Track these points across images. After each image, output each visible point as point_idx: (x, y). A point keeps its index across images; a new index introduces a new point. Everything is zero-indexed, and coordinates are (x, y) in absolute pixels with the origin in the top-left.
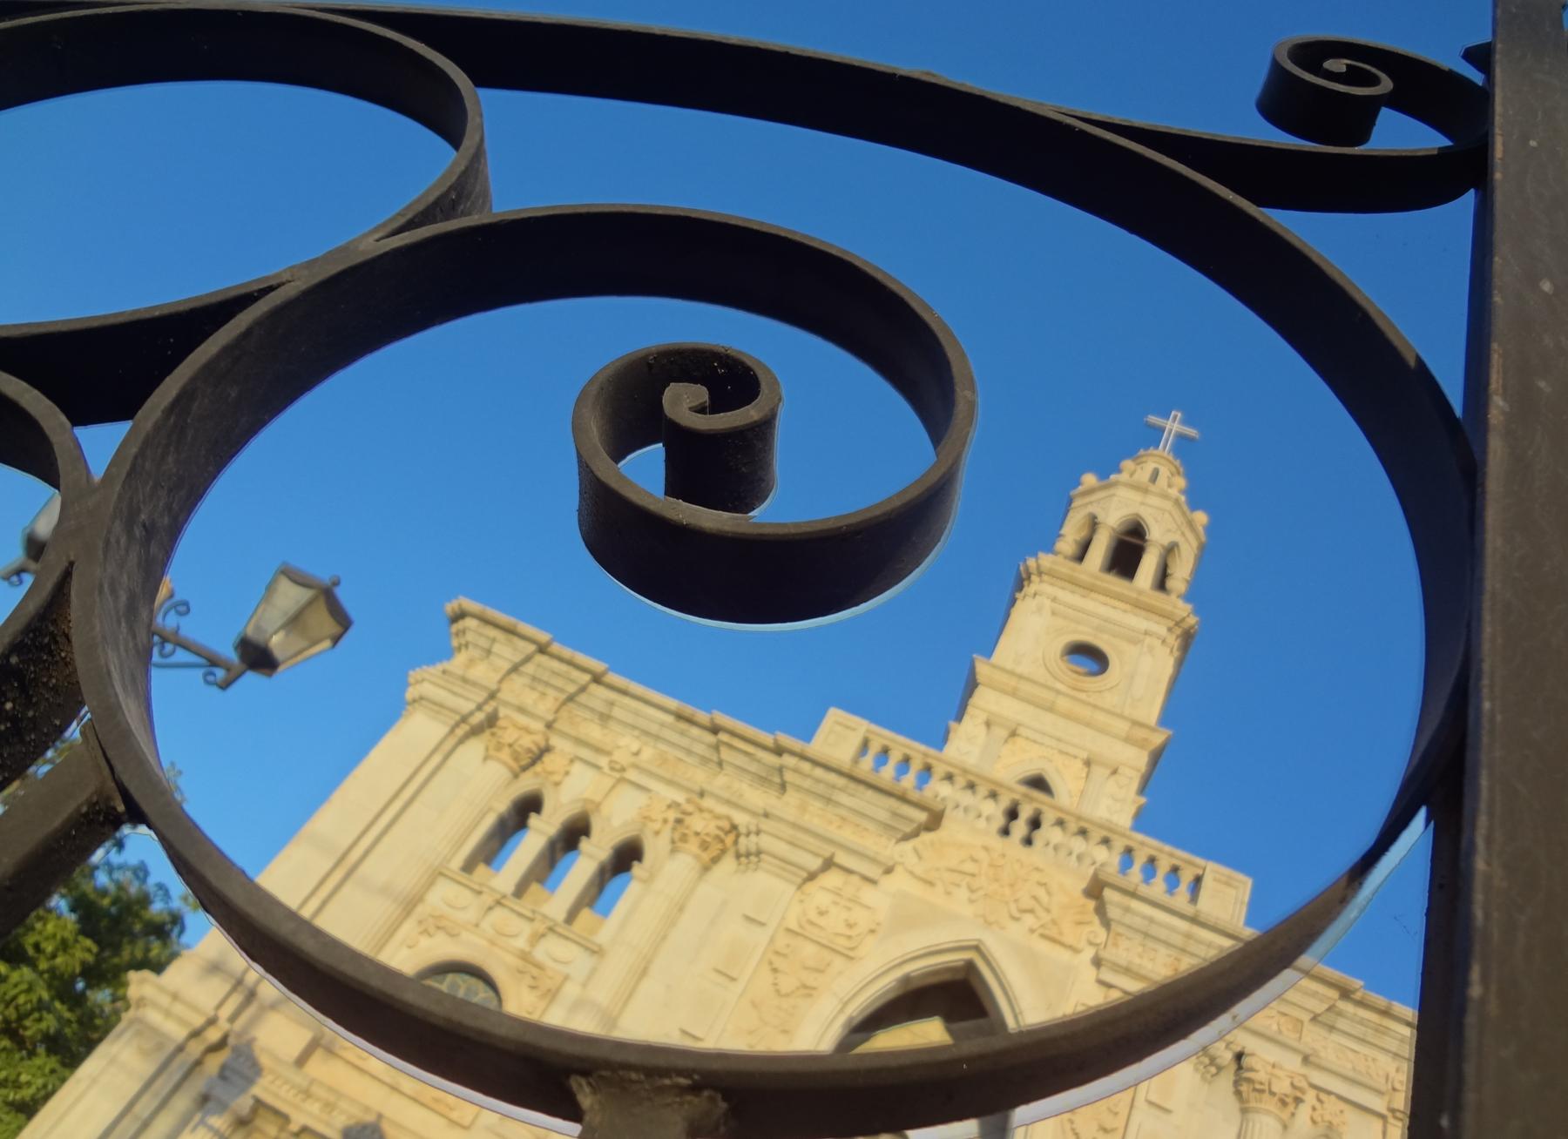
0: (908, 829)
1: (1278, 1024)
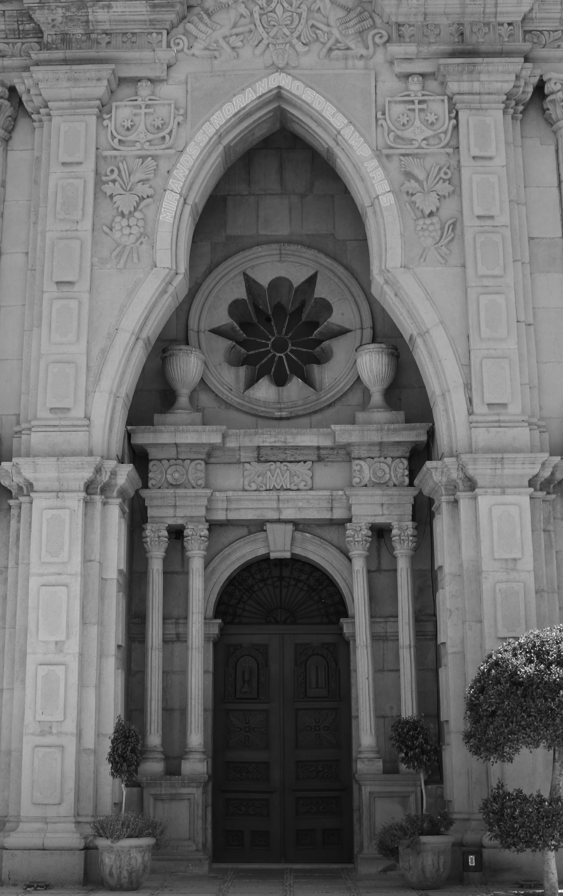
0: (172, 17)
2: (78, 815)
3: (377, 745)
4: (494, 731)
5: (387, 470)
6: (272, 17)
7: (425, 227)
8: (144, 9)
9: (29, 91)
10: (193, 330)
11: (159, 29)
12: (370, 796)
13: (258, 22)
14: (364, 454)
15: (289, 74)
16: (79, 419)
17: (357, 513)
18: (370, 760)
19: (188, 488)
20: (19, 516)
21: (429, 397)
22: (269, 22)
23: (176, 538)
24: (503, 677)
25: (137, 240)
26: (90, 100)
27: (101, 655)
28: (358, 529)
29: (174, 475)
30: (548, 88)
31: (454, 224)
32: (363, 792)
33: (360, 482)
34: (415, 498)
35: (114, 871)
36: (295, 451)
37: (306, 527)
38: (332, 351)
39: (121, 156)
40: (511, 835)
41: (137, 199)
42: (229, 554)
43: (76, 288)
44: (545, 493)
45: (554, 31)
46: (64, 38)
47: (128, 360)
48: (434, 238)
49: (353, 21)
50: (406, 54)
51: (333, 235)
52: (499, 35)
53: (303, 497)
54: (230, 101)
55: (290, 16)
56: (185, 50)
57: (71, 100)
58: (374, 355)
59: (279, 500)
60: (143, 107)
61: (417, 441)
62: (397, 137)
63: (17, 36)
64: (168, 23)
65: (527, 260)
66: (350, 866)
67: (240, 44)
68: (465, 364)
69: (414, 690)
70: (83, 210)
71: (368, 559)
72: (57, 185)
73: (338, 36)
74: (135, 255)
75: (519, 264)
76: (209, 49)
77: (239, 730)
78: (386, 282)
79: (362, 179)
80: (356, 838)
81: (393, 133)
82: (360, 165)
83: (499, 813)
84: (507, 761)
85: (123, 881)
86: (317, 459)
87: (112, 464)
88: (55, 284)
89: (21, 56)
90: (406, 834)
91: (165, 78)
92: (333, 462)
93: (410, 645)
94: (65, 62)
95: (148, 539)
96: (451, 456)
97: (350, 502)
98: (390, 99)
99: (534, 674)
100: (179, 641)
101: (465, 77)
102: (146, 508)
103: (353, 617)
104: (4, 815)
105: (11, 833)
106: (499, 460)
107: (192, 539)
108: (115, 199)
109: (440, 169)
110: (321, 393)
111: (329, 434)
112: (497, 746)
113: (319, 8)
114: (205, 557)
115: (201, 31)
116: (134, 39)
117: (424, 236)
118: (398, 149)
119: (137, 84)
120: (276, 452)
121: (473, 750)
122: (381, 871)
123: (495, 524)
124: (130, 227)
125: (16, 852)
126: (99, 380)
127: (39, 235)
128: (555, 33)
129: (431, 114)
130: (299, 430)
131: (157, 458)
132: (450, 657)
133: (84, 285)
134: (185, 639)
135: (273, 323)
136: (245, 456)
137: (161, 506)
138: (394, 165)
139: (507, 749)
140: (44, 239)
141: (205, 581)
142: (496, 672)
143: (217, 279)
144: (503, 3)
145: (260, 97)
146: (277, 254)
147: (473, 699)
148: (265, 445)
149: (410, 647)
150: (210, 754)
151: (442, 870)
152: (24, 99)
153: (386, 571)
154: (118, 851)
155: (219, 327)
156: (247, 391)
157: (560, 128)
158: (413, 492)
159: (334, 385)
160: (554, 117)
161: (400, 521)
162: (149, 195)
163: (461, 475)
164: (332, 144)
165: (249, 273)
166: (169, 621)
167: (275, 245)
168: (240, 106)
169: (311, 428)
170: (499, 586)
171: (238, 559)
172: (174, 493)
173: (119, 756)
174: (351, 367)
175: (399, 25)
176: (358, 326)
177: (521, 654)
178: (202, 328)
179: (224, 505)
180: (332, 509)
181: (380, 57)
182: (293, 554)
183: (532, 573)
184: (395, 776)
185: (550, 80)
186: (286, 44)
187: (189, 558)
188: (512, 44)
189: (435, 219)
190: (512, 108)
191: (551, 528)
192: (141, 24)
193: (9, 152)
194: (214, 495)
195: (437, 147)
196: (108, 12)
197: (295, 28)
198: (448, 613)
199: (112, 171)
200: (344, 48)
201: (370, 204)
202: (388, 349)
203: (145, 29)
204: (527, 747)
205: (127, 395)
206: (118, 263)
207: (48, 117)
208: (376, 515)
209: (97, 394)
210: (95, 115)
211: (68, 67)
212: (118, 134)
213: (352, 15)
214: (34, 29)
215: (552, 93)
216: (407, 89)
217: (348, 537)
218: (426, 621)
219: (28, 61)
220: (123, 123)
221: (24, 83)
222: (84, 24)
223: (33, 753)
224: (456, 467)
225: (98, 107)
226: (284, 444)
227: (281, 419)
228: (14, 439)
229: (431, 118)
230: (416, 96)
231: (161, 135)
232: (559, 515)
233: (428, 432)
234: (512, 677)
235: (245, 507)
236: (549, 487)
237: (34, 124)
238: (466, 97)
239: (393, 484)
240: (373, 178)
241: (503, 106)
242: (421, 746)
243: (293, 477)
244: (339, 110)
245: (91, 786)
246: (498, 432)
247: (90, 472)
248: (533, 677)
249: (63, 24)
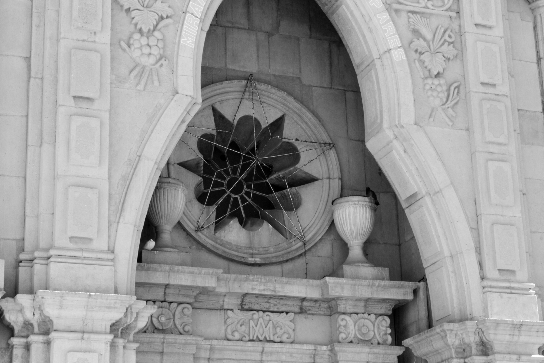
5: (371, 327)
7: (433, 87)
14: (350, 309)
16: (102, 252)
25: (157, 62)
33: (346, 338)
36: (278, 301)
41: (157, 17)
43: (96, 105)
48: (441, 99)
51: (299, 78)
58: (358, 208)
59: (262, 352)
68: (474, 227)
74: (155, 78)
79: (371, 31)
86: (299, 311)
88: (72, 98)
92: (313, 314)
106: (518, 326)
108: (134, 14)
109: (445, 32)
110: (291, 241)
117: (433, 96)
118: (406, 5)
120: (260, 300)
124: (150, 47)
136: (229, 302)
148: (254, 292)
157: (539, 7)
158: (399, 351)
162: (169, 15)
165: (218, 107)
172: (164, 338)
189: (442, 81)
195: (442, 9)
201: (378, 57)
206: (138, 84)
209: (121, 226)
224: (474, 330)
226: (273, 293)
235: (229, 357)
240: (385, 31)
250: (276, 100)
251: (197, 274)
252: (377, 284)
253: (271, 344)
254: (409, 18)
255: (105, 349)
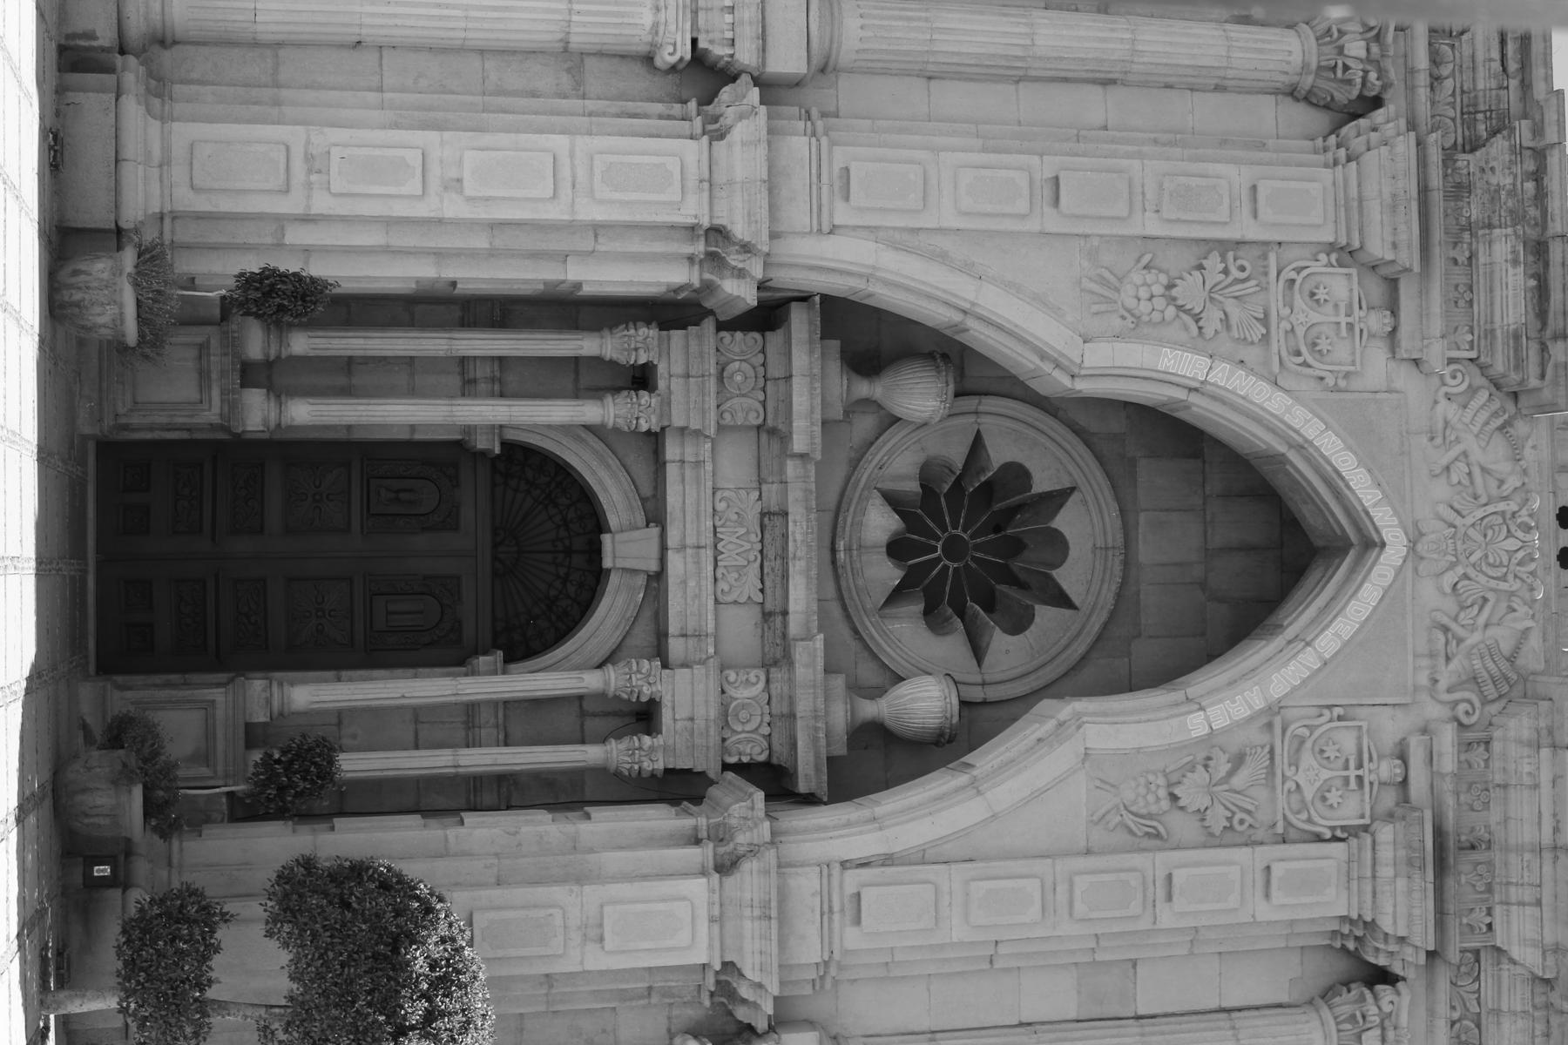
0: (1499, 367)
1: (1459, 1020)
2: (174, 218)
3: (293, 713)
4: (317, 905)
5: (748, 727)
6: (1500, 531)
7: (1153, 787)
8: (1511, 320)
9: (1375, 130)
10: (980, 403)
11: (1479, 346)
12: (208, 701)
13: (1490, 509)
14: (776, 688)
15: (1404, 561)
16: (831, 215)
17: (677, 678)
18: (269, 701)
19: (717, 397)
20: (670, 117)
21: (871, 796)
22: (1491, 527)
23: (634, 377)
24: (406, 921)
25: (1129, 311)
26: (1361, 231)
27: (439, 255)
28: (651, 680)
29: (740, 372)
30: (1385, 991)
31: (1158, 836)
32: (215, 690)
33: (729, 683)
34: (702, 774)
35: (82, 278)
36: (780, 573)
37: (654, 593)
38: (947, 634)
39: (1268, 283)
40: (145, 935)
41: (1197, 310)
42: (608, 467)
43: (1048, 210)
44: (713, 989)
45: (1478, 999)
46: (1463, 187)
47: (929, 297)
48: (1135, 802)
49: (1494, 666)
50: (1440, 755)
51: (1139, 635)
52: (1472, 909)
53: (703, 588)
54: (1361, 463)
55: (1501, 562)
56: (1445, 389)
57: (1361, 200)
58: (939, 704)
59: (699, 547)
60: (1350, 320)
61: (797, 778)
62: (1302, 741)
63: (1465, 110)
64: (1489, 360)
65: (1098, 957)
66: (92, 668)
67: (1455, 479)
68: (926, 855)
69: (385, 773)
70: (1178, 221)
71: (601, 696)
72: (1218, 177)
73: (1469, 642)
74: (1103, 307)
75: (1093, 944)
76: (1445, 428)
77: (317, 483)
78: (1061, 724)
79: (1231, 683)
80: (138, 679)
81: (1308, 734)
82: (1255, 679)
83: (181, 916)
84: (268, 928)
85: (65, 292)
86: (767, 611)
87: (758, 272)
88: (1054, 175)
89: (1433, 116)
90: (145, 761)
91: (1398, 356)
92: (762, 637)
93: (459, 766)
94: (1424, 190)
95: (632, 332)
96: (773, 834)
97: (695, 667)
98: (1365, 729)
99: (412, 972)
100: (464, 384)
101: (1402, 853)
102: (684, 328)
103: (504, 672)
104: (174, 96)
105: (144, 107)
107: (632, 404)
108: (1197, 274)
109: (1249, 812)
110: (877, 616)
111: (808, 630)
112: (292, 912)
113: (1514, 610)
114: (603, 426)
115: (1475, 415)
116: (1461, 303)
117: (1138, 786)
119: (1387, 309)
120: (778, 543)
121: (286, 872)
122: (84, 720)
123: (661, 906)
124: (1150, 300)
125: (113, 115)
126: (897, 249)
127: (1136, 148)
128: (1475, 1002)
129: (1341, 796)
130: (815, 581)
131: (768, 345)
132: (440, 832)
133: (1053, 223)
134: (466, 393)
135: (992, 536)
136: (772, 491)
137: (687, 353)
138: (1255, 736)
139: (287, 928)
140: (1128, 156)
141: (563, 426)
142: (416, 909)
143: (1065, 444)
144: (1524, 915)
145: (1367, 513)
146: (1106, 542)
147: (371, 872)
148: (790, 524)
149: (455, 767)
150: (277, 436)
151: (86, 821)
152: (1361, 121)
153: (582, 725)
154: (115, 284)
155: (984, 447)
156: (879, 494)
157: (1317, 1011)
158: (713, 769)
159: (890, 639)
160: (1337, 1000)
161: (665, 748)
162: (1203, 331)
163: (742, 849)
164: (1290, 633)
165: (1075, 497)
166: (496, 367)
167: (1122, 540)
168: (1353, 480)
169: (819, 600)
170: (557, 913)
171: (600, 482)
173: (272, 285)
174: (919, 665)
175: (1487, 743)
176: (988, 678)
177: (446, 950)
178: (984, 419)
179: (689, 458)
180: (685, 636)
181: (1434, 711)
182: (609, 571)
183: (579, 969)
184: (242, 743)
185: (1398, 993)
186: (1456, 557)
187: (601, 399)
188: (1457, 931)
189: (1165, 804)
190: (1351, 930)
191: (654, 1000)
192: (1486, 316)
193: (1273, 97)
194: (707, 440)
195: (1286, 807)
196: (1506, 261)
197: (1481, 571)
198: (513, 830)
199: (1242, 269)
200: (1449, 651)
201: (1190, 697)
202: (951, 729)
203: (1479, 322)
204: (290, 961)
205: (870, 295)
206: (1090, 279)
207: (1331, 161)
208: (674, 709)
209: (872, 245)
210: (1336, 239)
211: (1414, 193)
212: (1304, 278)
213: (1504, 666)
214: (1478, 138)
215: (1376, 998)
216: (1381, 757)
217: (638, 664)
218: (499, 791)
219: (1425, 128)
220: (1322, 287)
221: (1388, 122)
222: (1487, 221)
223: (277, 143)
224: (755, 842)
225: (1348, 244)
226: (791, 555)
227: (833, 550)
228: (797, 109)
229: (1333, 797)
230: (1370, 771)
231: (1304, 349)
232: (676, 1012)
233: (812, 795)
234: (407, 937)
236: (722, 996)
237: (1321, 139)
238: (1369, 854)
239: (726, 736)
241: (1355, 916)
242: (292, 785)
243: (737, 571)
244: (1346, 644)
245: (223, 239)
246: (813, 911)
247: (743, 234)
248: (408, 971)
249: (1486, 187)
250: (1099, 593)
251: (811, 418)
252: (819, 725)
253: (711, 559)
254: (1263, 747)
255: (685, 216)
